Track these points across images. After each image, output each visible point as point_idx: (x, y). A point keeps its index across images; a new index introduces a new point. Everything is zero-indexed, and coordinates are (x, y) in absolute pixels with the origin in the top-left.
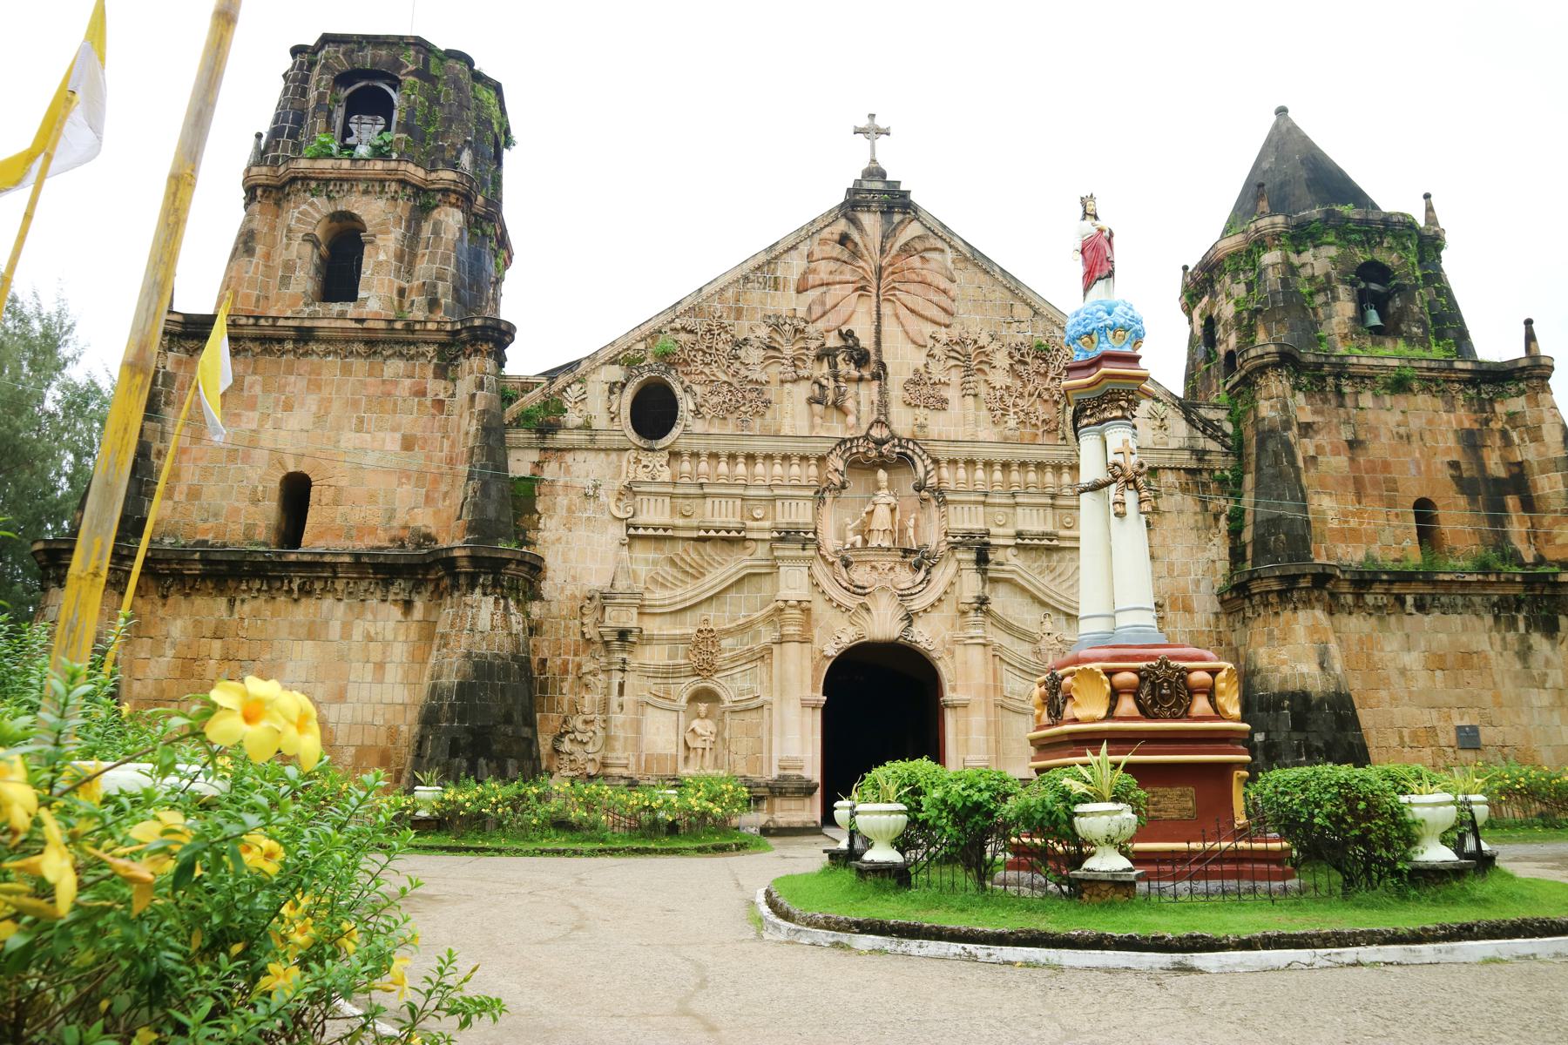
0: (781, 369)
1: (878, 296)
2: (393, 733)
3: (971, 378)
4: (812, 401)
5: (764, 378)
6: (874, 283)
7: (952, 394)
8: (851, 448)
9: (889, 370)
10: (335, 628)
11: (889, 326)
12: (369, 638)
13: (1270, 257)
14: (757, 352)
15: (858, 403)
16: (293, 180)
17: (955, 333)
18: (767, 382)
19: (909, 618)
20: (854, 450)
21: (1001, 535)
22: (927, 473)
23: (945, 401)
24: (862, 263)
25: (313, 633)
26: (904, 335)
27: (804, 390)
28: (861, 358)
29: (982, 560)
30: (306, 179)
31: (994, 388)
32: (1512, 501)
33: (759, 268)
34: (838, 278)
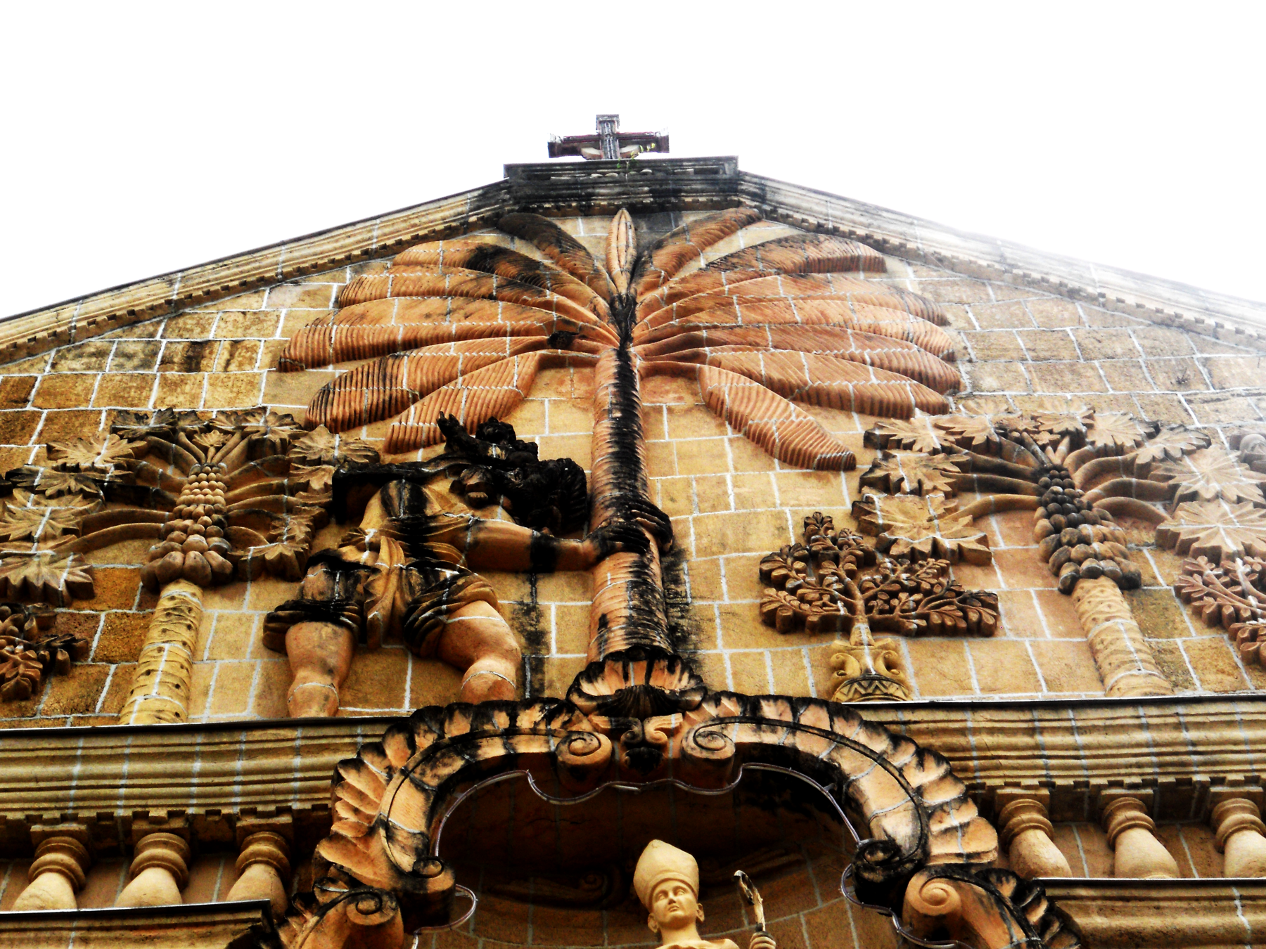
0: (155, 546)
1: (623, 355)
3: (1087, 529)
5: (63, 575)
6: (612, 331)
8: (467, 743)
9: (690, 540)
14: (53, 505)
15: (536, 639)
18: (81, 592)
20: (493, 750)
22: (924, 814)
23: (988, 602)
24: (556, 298)
26: (750, 447)
31: (1215, 555)
33: (131, 319)
34: (453, 326)
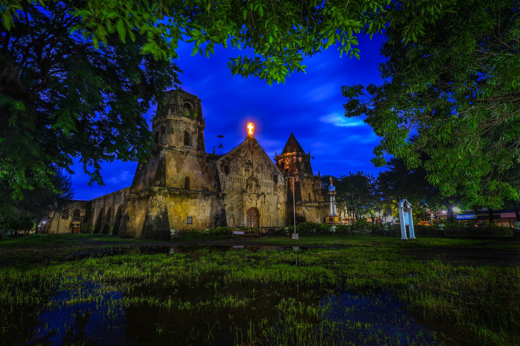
2: (206, 220)
4: (245, 170)
7: (260, 171)
10: (198, 204)
11: (254, 160)
12: (202, 206)
13: (295, 158)
16: (180, 120)
17: (261, 162)
19: (256, 204)
21: (266, 193)
25: (195, 205)
27: (244, 169)
28: (251, 164)
29: (265, 196)
30: (182, 121)
32: (316, 194)
